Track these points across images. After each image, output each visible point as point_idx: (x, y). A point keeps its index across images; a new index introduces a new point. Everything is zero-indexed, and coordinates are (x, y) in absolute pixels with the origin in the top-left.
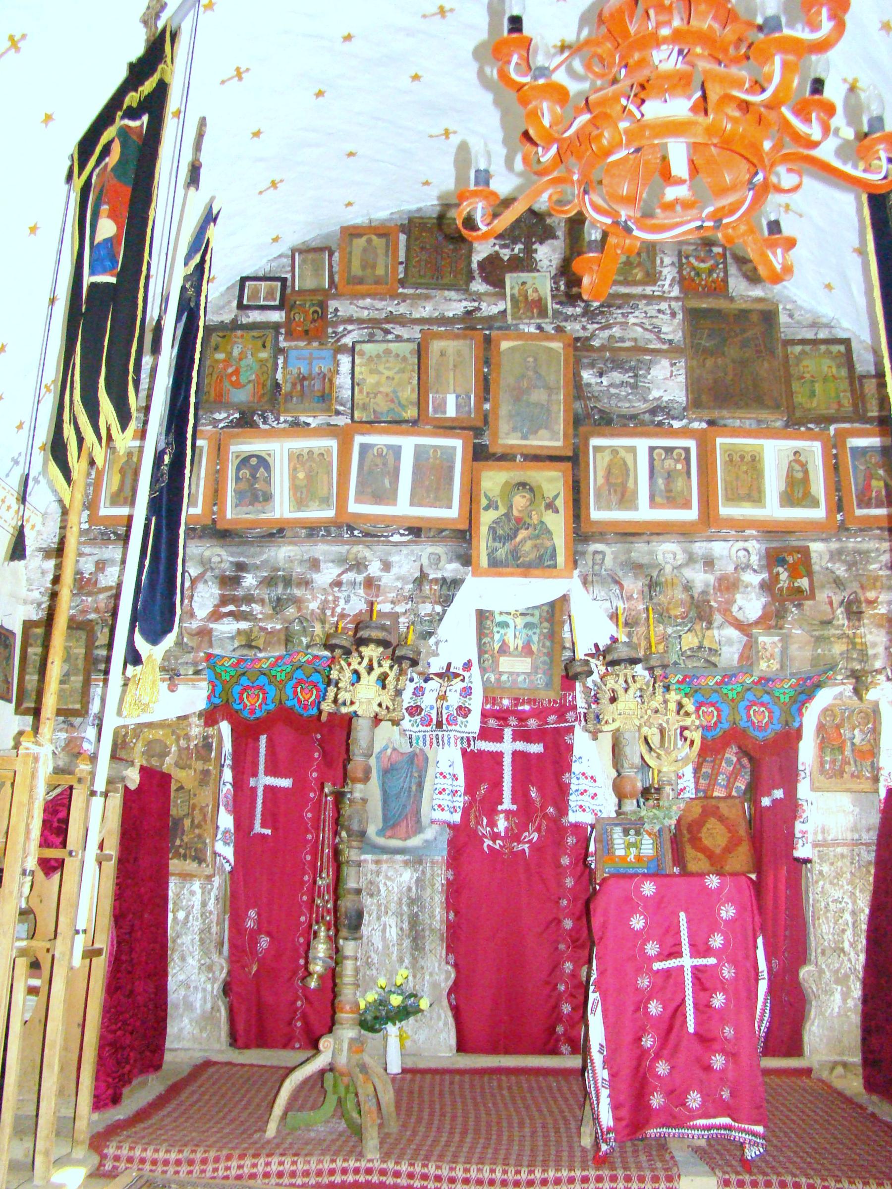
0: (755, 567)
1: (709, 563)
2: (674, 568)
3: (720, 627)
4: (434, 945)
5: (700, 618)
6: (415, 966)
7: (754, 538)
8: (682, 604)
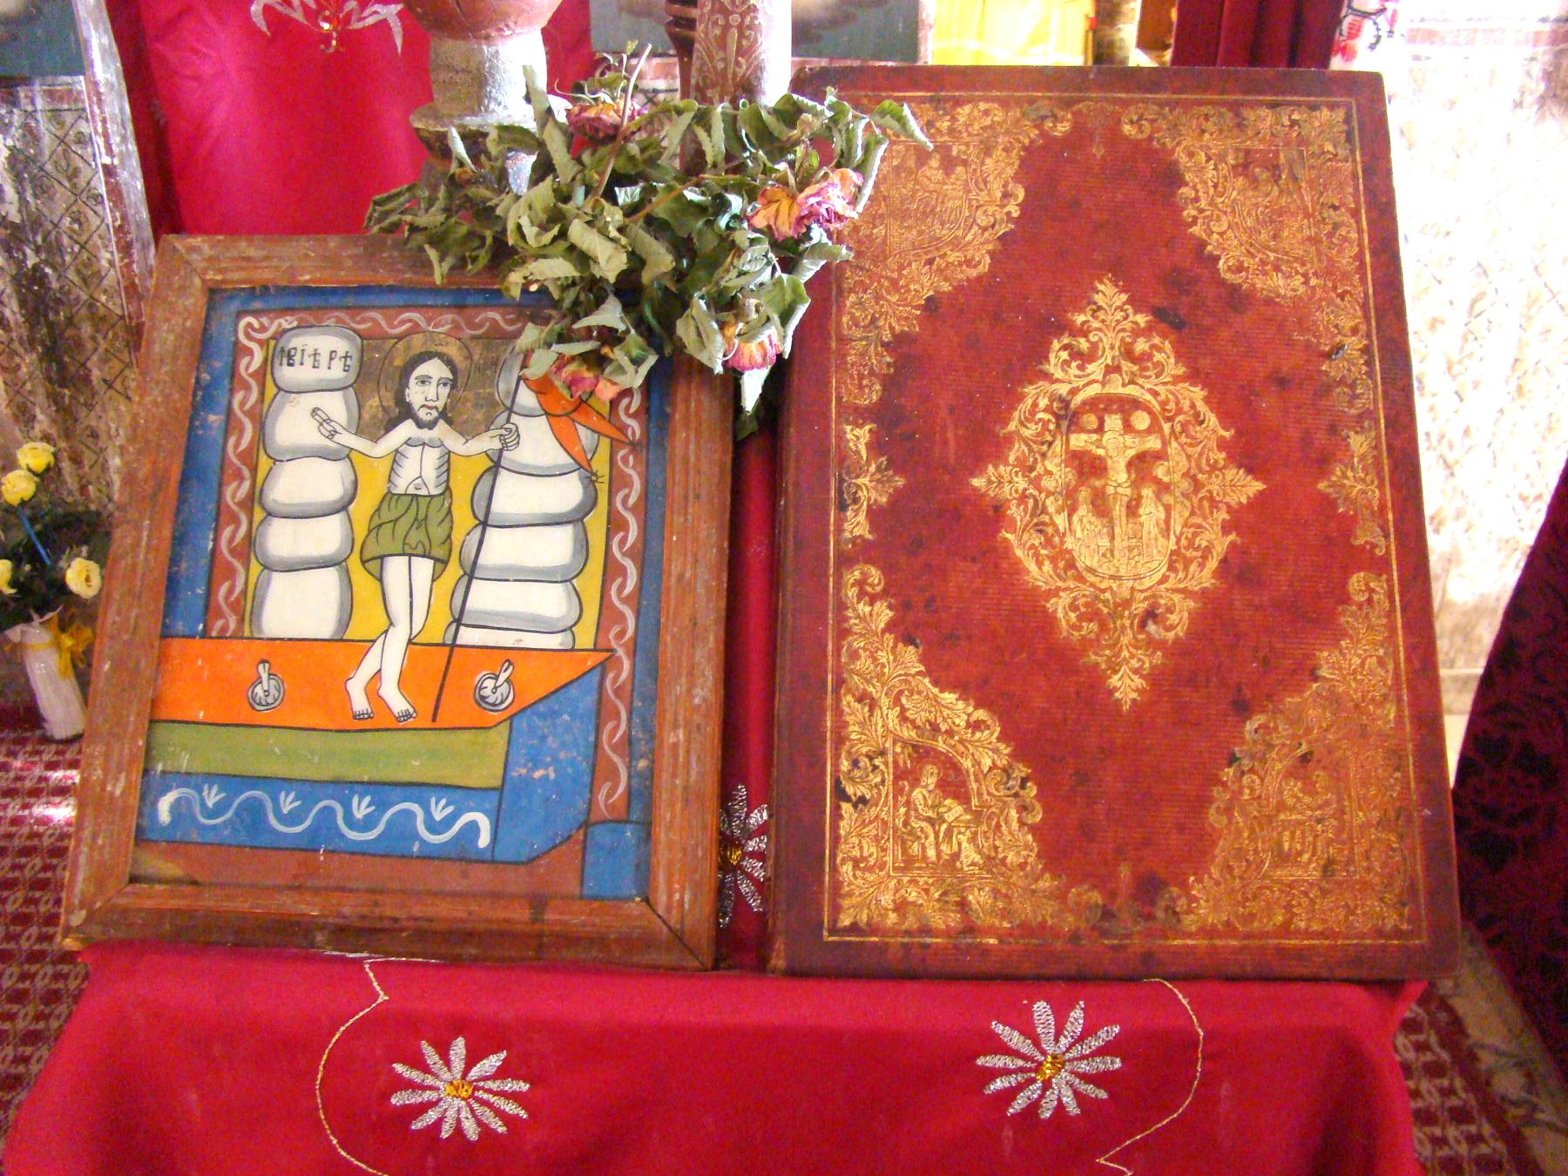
4: (116, 365)
6: (70, 429)
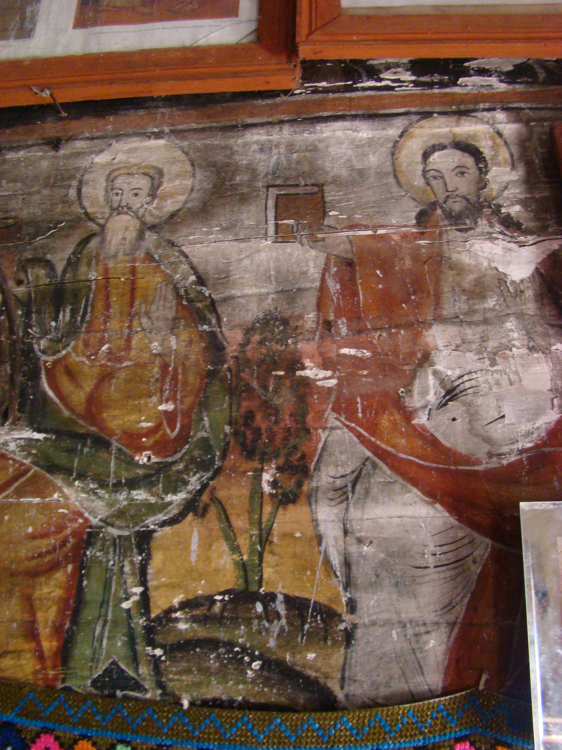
0: (515, 210)
1: (302, 202)
2: (146, 227)
3: (348, 491)
5: (250, 444)
7: (496, 102)
8: (169, 373)
